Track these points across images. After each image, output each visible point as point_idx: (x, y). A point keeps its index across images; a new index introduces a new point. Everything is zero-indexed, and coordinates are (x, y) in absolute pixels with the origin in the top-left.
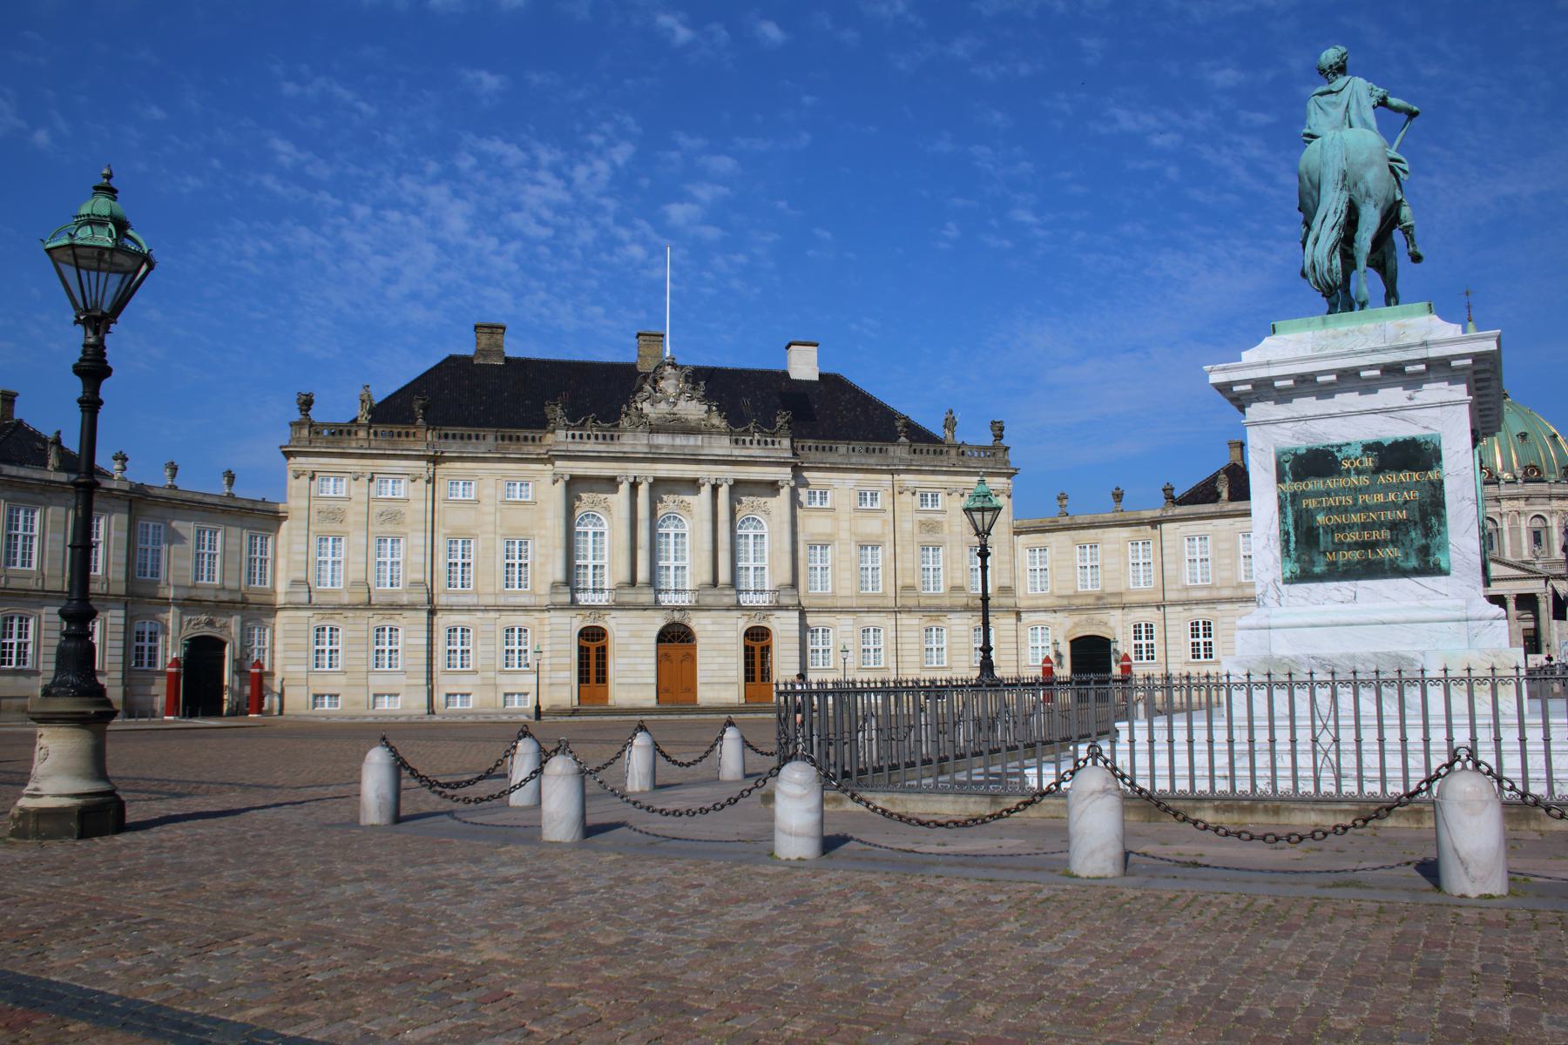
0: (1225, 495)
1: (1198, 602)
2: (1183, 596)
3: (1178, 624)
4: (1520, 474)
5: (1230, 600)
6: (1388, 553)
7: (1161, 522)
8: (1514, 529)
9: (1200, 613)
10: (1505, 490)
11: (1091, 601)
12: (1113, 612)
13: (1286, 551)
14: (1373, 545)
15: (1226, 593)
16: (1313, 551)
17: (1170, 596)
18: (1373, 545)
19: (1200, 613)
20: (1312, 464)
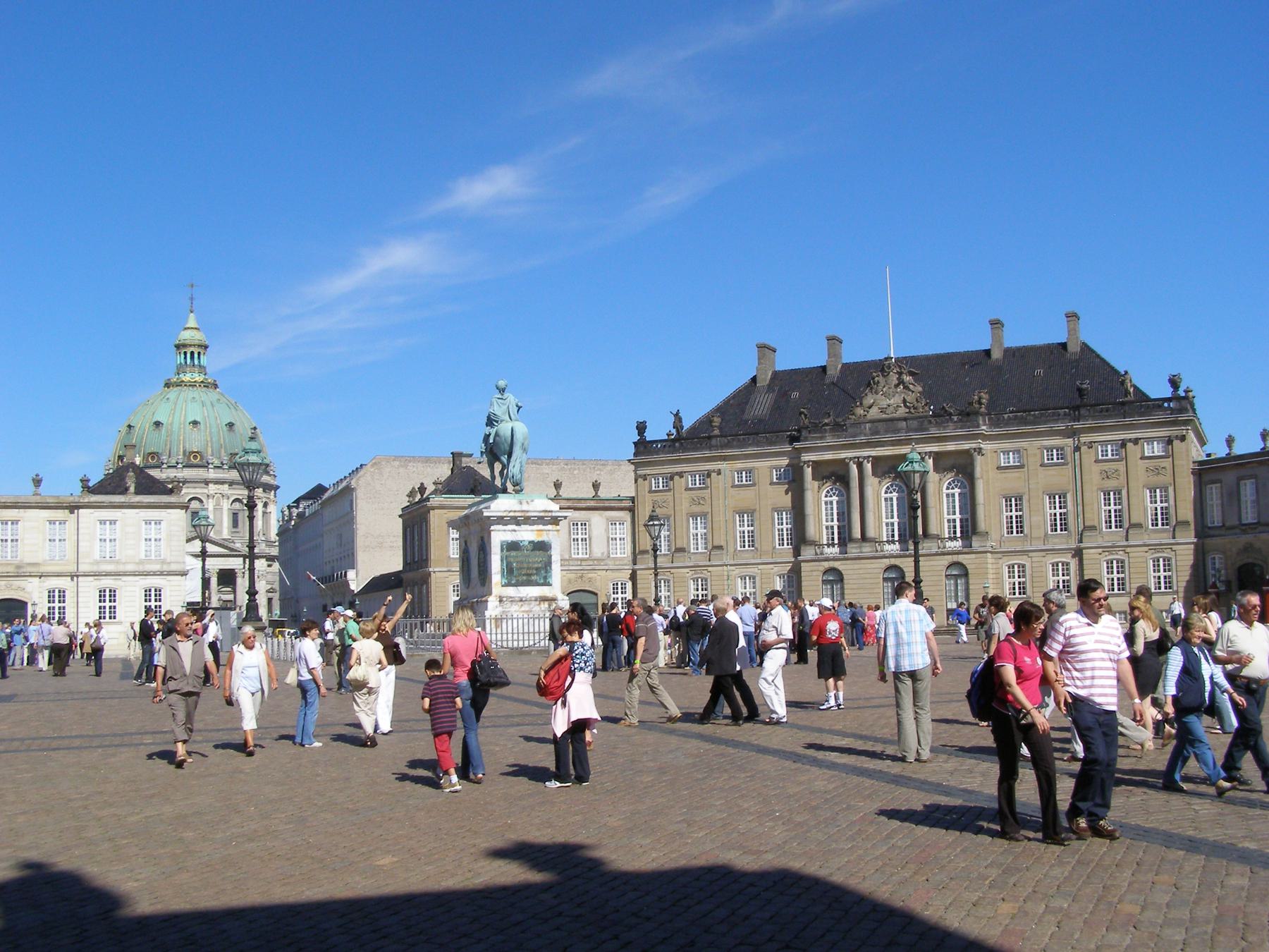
0: (132, 489)
1: (108, 574)
2: (95, 568)
3: (89, 589)
4: (226, 459)
5: (134, 574)
6: (533, 578)
7: (78, 507)
8: (218, 509)
9: (107, 583)
10: (212, 474)
11: (11, 569)
12: (30, 579)
13: (503, 575)
14: (530, 575)
15: (130, 568)
16: (515, 576)
17: (84, 568)
18: (530, 575)
19: (107, 583)
20: (512, 546)
